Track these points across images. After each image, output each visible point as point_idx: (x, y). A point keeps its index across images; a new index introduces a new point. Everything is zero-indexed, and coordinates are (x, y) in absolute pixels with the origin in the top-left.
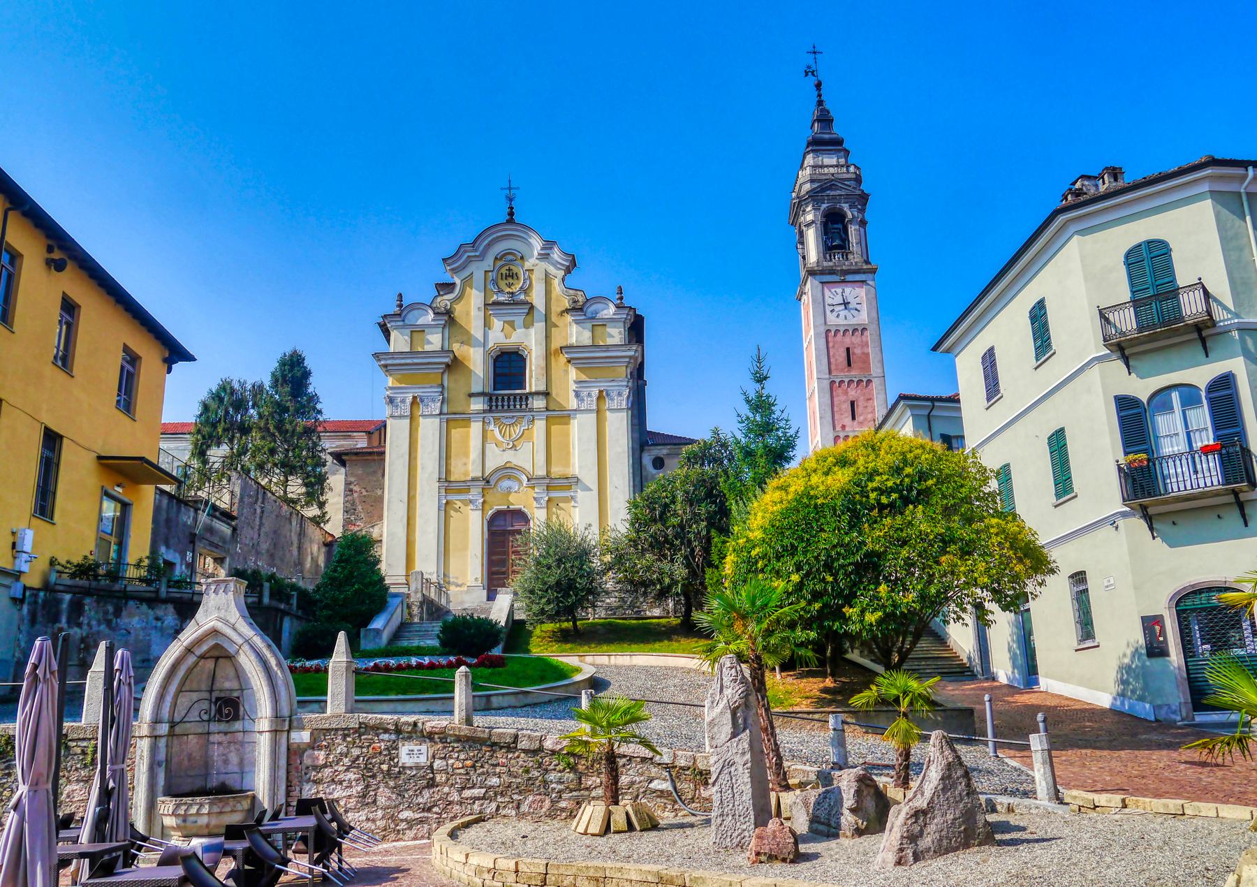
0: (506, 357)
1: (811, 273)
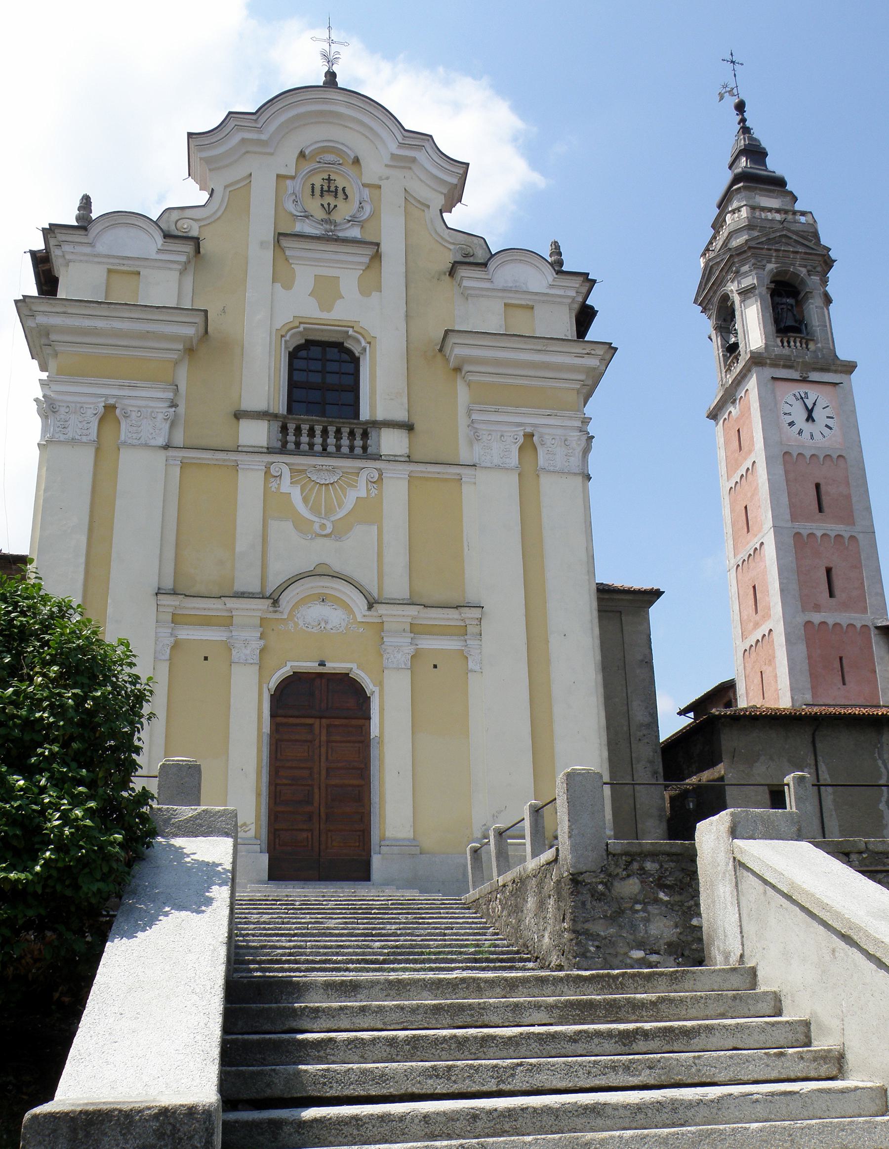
0: (316, 352)
1: (757, 360)
